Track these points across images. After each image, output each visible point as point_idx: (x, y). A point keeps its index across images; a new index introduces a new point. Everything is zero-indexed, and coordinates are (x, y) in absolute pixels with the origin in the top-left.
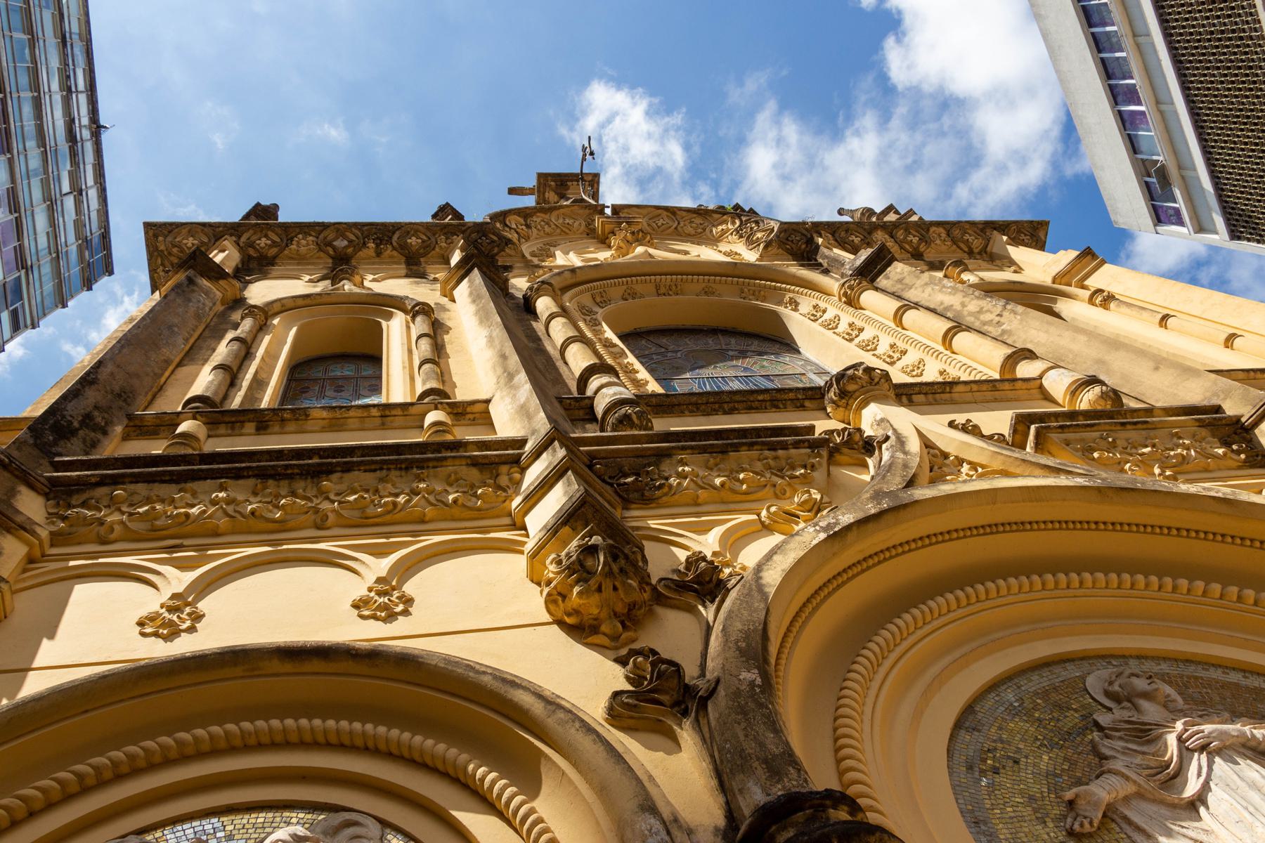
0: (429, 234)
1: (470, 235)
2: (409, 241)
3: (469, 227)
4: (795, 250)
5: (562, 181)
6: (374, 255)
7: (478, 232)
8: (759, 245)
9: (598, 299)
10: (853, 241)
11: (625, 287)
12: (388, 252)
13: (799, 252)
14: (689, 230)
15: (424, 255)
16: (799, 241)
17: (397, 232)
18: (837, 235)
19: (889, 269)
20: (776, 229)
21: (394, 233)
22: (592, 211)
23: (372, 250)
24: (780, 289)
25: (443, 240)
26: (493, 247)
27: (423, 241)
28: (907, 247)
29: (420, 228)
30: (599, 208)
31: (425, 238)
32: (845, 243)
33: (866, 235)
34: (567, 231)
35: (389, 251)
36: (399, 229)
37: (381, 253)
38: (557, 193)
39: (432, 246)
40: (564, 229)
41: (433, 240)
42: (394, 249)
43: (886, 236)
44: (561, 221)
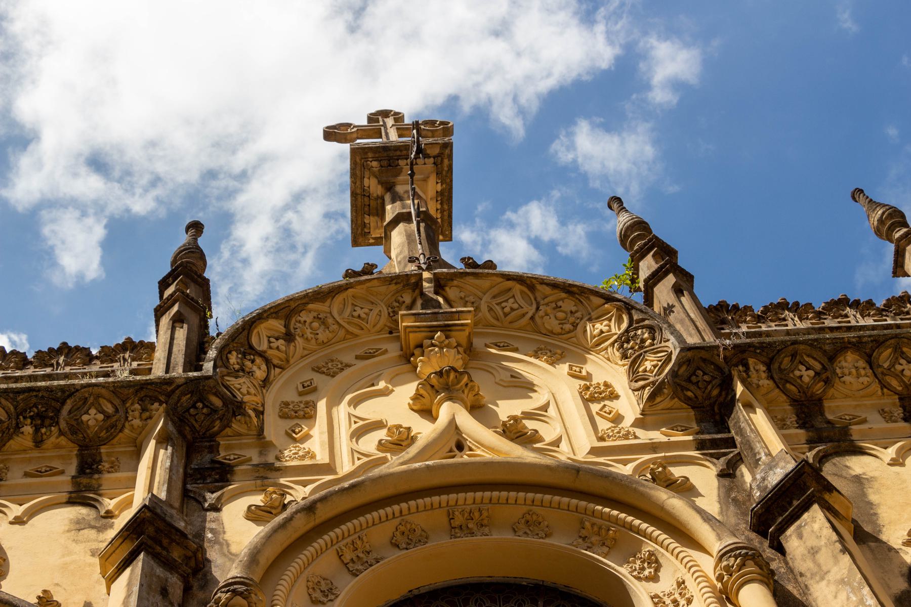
0: (117, 402)
1: (179, 400)
2: (85, 418)
3: (179, 386)
4: (700, 398)
5: (390, 159)
6: (30, 443)
7: (192, 392)
8: (643, 387)
9: (347, 557)
10: (801, 377)
11: (397, 521)
12: (53, 439)
13: (707, 402)
14: (552, 324)
15: (105, 442)
16: (709, 383)
17: (68, 401)
18: (775, 366)
19: (805, 516)
20: (674, 357)
21: (63, 403)
22: (400, 286)
23: (29, 438)
24: (638, 531)
25: (137, 414)
26: (213, 421)
27: (107, 417)
28: (894, 383)
29: (103, 391)
30: (413, 280)
31: (109, 409)
32: (787, 381)
33: (825, 360)
34: (356, 331)
35: (53, 438)
36: (69, 396)
37: (42, 441)
38: (380, 182)
39: (119, 426)
40: (351, 329)
41: (121, 413)
42: (61, 433)
43: (861, 363)
44: (348, 310)
